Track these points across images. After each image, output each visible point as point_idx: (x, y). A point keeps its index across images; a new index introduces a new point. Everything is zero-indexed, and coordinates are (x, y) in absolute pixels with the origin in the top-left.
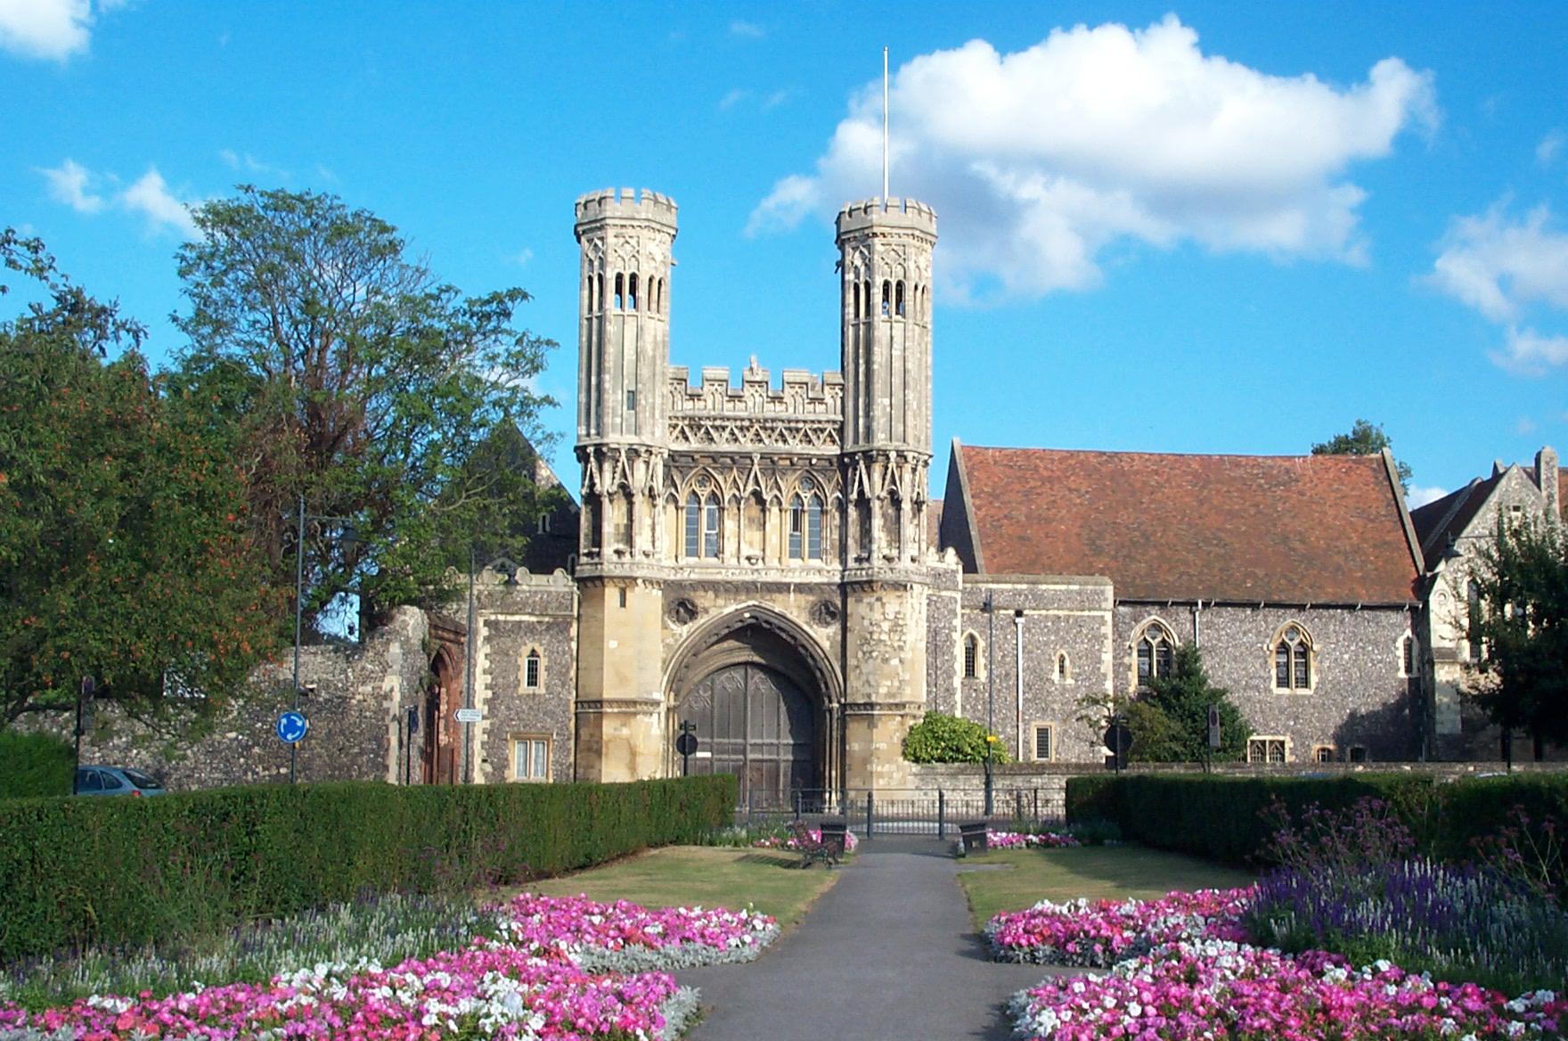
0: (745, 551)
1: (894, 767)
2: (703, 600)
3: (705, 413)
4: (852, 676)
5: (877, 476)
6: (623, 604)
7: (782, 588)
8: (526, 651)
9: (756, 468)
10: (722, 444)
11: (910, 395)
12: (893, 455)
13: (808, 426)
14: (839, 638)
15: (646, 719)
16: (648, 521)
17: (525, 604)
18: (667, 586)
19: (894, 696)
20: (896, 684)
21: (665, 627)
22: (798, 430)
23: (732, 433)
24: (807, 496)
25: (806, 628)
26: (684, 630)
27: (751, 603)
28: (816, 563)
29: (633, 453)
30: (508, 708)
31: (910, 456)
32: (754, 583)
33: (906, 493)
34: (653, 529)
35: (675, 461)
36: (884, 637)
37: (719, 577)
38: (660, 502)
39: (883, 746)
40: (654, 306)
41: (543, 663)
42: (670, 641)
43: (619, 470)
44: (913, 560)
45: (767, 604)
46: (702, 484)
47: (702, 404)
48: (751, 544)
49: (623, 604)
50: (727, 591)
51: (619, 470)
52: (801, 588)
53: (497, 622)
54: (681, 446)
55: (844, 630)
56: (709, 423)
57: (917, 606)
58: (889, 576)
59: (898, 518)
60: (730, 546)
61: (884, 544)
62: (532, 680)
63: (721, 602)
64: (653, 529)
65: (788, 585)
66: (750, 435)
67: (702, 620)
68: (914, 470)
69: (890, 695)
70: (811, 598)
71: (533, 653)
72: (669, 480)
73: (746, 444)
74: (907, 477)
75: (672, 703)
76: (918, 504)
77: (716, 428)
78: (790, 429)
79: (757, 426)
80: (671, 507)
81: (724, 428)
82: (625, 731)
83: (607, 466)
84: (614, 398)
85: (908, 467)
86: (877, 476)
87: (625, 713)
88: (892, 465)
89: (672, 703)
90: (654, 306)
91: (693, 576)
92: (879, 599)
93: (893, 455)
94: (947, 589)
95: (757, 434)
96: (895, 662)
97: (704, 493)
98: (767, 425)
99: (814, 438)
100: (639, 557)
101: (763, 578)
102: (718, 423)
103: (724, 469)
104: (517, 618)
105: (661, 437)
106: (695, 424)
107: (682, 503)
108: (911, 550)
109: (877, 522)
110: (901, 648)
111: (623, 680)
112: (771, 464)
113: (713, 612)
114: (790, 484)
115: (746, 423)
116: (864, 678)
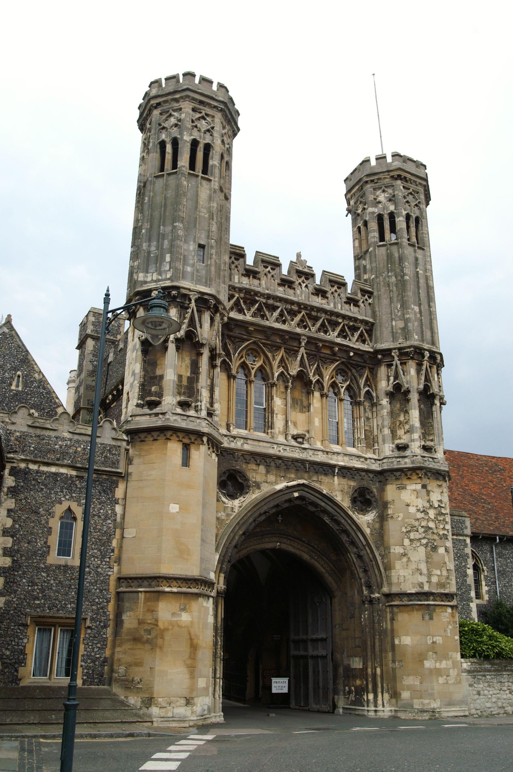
1: (450, 663)
2: (256, 473)
4: (398, 565)
7: (327, 469)
8: (59, 510)
9: (302, 350)
10: (272, 322)
12: (427, 354)
17: (64, 454)
20: (445, 573)
27: (301, 481)
32: (303, 462)
36: (431, 525)
39: (439, 640)
42: (222, 515)
45: (316, 485)
47: (256, 282)
50: (278, 467)
52: (346, 472)
53: (27, 472)
60: (279, 422)
62: (64, 549)
63: (271, 478)
65: (333, 466)
70: (353, 484)
73: (291, 326)
77: (268, 306)
78: (329, 321)
82: (185, 617)
87: (185, 594)
88: (426, 364)
91: (246, 447)
93: (427, 354)
102: (271, 302)
104: (53, 469)
111: (183, 553)
113: (266, 489)
115: (295, 308)
116: (413, 566)
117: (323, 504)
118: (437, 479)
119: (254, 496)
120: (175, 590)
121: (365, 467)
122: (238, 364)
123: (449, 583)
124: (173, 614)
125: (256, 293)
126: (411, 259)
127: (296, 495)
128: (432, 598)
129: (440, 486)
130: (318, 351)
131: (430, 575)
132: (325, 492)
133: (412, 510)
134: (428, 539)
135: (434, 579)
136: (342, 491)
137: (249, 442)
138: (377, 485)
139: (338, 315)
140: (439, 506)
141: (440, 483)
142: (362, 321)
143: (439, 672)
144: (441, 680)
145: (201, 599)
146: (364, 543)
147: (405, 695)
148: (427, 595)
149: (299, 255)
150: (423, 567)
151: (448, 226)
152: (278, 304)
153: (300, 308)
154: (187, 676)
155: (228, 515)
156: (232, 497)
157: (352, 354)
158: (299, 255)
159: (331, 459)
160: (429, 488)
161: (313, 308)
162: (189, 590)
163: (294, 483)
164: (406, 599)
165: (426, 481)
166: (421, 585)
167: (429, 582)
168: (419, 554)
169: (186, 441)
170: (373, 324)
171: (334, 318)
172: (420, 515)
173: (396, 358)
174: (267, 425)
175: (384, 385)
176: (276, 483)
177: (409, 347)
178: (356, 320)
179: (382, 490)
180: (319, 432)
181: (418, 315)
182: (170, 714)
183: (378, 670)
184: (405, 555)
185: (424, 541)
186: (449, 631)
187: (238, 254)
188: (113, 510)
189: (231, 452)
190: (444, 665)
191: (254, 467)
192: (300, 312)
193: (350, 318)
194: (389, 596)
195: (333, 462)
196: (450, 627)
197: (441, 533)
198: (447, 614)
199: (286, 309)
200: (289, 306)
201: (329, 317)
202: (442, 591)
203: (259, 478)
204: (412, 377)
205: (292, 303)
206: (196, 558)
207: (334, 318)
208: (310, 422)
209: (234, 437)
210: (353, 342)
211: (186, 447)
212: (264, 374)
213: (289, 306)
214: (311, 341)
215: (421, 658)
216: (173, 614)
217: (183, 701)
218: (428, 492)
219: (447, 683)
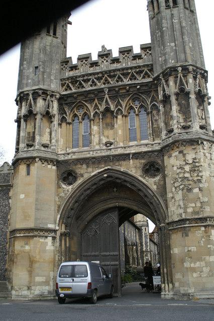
0: (104, 140)
1: (203, 263)
3: (78, 74)
4: (170, 204)
6: (28, 174)
7: (125, 157)
10: (88, 87)
11: (186, 38)
13: (133, 71)
14: (162, 183)
15: (42, 240)
16: (48, 130)
18: (58, 163)
19: (198, 213)
20: (199, 205)
21: (59, 187)
22: (128, 74)
25: (140, 178)
26: (69, 189)
27: (106, 168)
31: (191, 68)
32: (108, 156)
34: (51, 134)
35: (62, 100)
36: (187, 175)
38: (56, 121)
39: (193, 249)
42: (62, 194)
43: (28, 104)
45: (117, 168)
47: (77, 71)
49: (28, 174)
50: (93, 163)
51: (28, 104)
52: (136, 156)
54: (69, 92)
55: (164, 177)
56: (81, 79)
58: (186, 137)
59: (188, 104)
60: (95, 139)
61: (181, 120)
63: (90, 170)
64: (51, 134)
65: (129, 154)
67: (80, 181)
68: (195, 78)
69: (194, 213)
70: (143, 161)
72: (62, 111)
73: (100, 85)
74: (191, 81)
75: (63, 230)
78: (123, 74)
79: (106, 76)
82: (27, 248)
88: (180, 75)
89: (63, 230)
91: (74, 157)
92: (181, 152)
93: (180, 69)
95: (106, 80)
96: (196, 190)
98: (111, 74)
101: (114, 152)
102: (86, 78)
103: (91, 101)
106: (74, 80)
109: (175, 108)
110: (200, 181)
111: (26, 217)
113: (86, 176)
115: (100, 75)
116: (177, 204)
117: (123, 177)
118: (192, 145)
119: (80, 181)
120: (22, 235)
121: (150, 149)
122: (71, 116)
123: (202, 211)
124: (22, 246)
125: (76, 77)
126: (169, 16)
127: (105, 175)
128: (188, 222)
129: (194, 149)
130: (115, 94)
131: (186, 208)
132: (122, 170)
133: (175, 168)
134: (185, 185)
135: (190, 210)
136: (135, 167)
137: (76, 154)
138: (162, 158)
139: (127, 69)
140: (193, 162)
141: (193, 147)
142: (144, 66)
143: (193, 270)
144: (195, 275)
145: (35, 238)
146: (152, 195)
147: (177, 284)
148: (183, 221)
149: (103, 47)
150: (181, 203)
152: (90, 77)
153: (103, 74)
154: (28, 276)
155: (66, 194)
156: (70, 184)
157: (138, 87)
158: (103, 47)
159: (126, 151)
160: (185, 152)
161: (110, 71)
162: (29, 235)
163: (103, 169)
164: (175, 225)
165: (182, 148)
166: (181, 215)
167: (185, 212)
168: (179, 196)
169: (28, 163)
170: (152, 65)
171: (125, 71)
172: (179, 171)
173: (163, 79)
175: (161, 97)
176: (93, 172)
177: (167, 69)
178: (139, 67)
179: (163, 161)
180: (119, 138)
181: (174, 48)
182: (20, 294)
183: (165, 270)
184: (173, 198)
185: (181, 187)
186: (202, 243)
188: (8, 202)
189: (66, 162)
190: (198, 264)
191: (80, 166)
192: (104, 77)
193: (135, 67)
195: (128, 152)
196: (203, 240)
197: (195, 179)
198: (200, 232)
199: (95, 78)
200: (96, 76)
201: (121, 72)
202: (196, 217)
204: (191, 85)
205: (98, 73)
206: (33, 218)
207: (125, 71)
208: (116, 133)
209: (68, 154)
210: (140, 80)
211: (28, 166)
213: (96, 76)
214: (111, 89)
215: (183, 261)
216: (22, 246)
217: (26, 288)
218: (184, 155)
219: (200, 276)
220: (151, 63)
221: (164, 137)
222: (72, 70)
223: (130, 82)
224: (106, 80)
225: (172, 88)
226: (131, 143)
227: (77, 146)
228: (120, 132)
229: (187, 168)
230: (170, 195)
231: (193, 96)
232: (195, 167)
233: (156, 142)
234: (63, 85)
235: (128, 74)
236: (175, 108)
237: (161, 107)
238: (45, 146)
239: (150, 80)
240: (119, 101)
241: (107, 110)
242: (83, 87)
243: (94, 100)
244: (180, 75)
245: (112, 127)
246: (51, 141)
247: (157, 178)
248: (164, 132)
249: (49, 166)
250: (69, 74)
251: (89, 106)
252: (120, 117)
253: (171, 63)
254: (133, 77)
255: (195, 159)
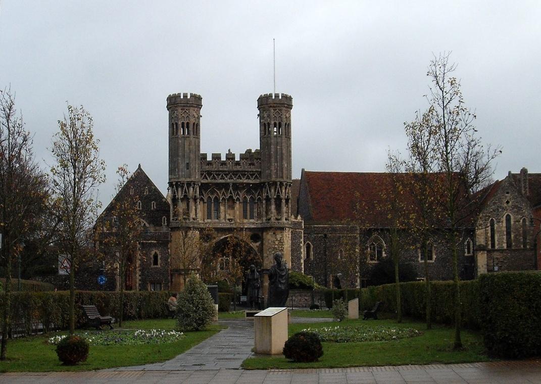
0: (228, 217)
5: (273, 191)
8: (153, 253)
9: (231, 188)
16: (194, 208)
18: (201, 230)
23: (222, 176)
24: (248, 198)
28: (252, 221)
29: (189, 184)
30: (148, 272)
33: (283, 196)
34: (196, 211)
35: (204, 187)
37: (219, 226)
38: (198, 200)
40: (195, 133)
41: (159, 257)
44: (286, 220)
46: (212, 194)
48: (230, 215)
50: (222, 231)
51: (184, 190)
54: (205, 181)
55: (262, 244)
57: (287, 235)
60: (222, 215)
61: (276, 214)
63: (219, 235)
64: (196, 211)
66: (228, 177)
68: (286, 188)
71: (156, 253)
72: (201, 193)
73: (227, 180)
74: (284, 191)
76: (287, 200)
80: (202, 202)
81: (219, 175)
83: (180, 189)
84: (182, 166)
85: (284, 188)
86: (273, 191)
88: (278, 186)
90: (195, 133)
94: (298, 229)
95: (231, 176)
97: (213, 197)
98: (235, 173)
99: (251, 177)
100: (191, 220)
102: (217, 173)
103: (220, 189)
104: (150, 242)
105: (196, 177)
106: (209, 173)
107: (206, 201)
108: (285, 216)
112: (236, 187)
113: (217, 239)
114: (242, 194)
115: (227, 173)
133: (270, 241)
139: (245, 171)
149: (229, 150)
151: (298, 117)
158: (229, 150)
160: (276, 233)
161: (234, 171)
172: (272, 243)
174: (218, 217)
175: (264, 195)
176: (221, 236)
179: (262, 234)
184: (267, 257)
187: (204, 156)
188: (168, 251)
194: (263, 270)
197: (280, 249)
203: (214, 236)
205: (226, 171)
208: (234, 213)
212: (217, 199)
214: (234, 184)
218: (276, 235)
220: (260, 170)
221: (264, 221)
222: (208, 165)
223: (245, 181)
224: (231, 176)
225: (273, 194)
226: (245, 221)
227: (211, 219)
228: (238, 213)
229: (277, 243)
230: (265, 255)
231: (284, 201)
232: (281, 242)
233: (259, 222)
234: (202, 175)
235: (245, 175)
236: (273, 207)
237: (264, 202)
238: (194, 219)
239: (258, 181)
240: (238, 192)
241: (231, 197)
242: (215, 179)
243: (222, 189)
244: (278, 186)
245: (233, 208)
246: (196, 215)
247: (258, 244)
248: (264, 219)
249: (197, 232)
250: (207, 168)
251: (218, 192)
252: (238, 202)
253: (273, 178)
254: (248, 178)
255: (281, 238)
